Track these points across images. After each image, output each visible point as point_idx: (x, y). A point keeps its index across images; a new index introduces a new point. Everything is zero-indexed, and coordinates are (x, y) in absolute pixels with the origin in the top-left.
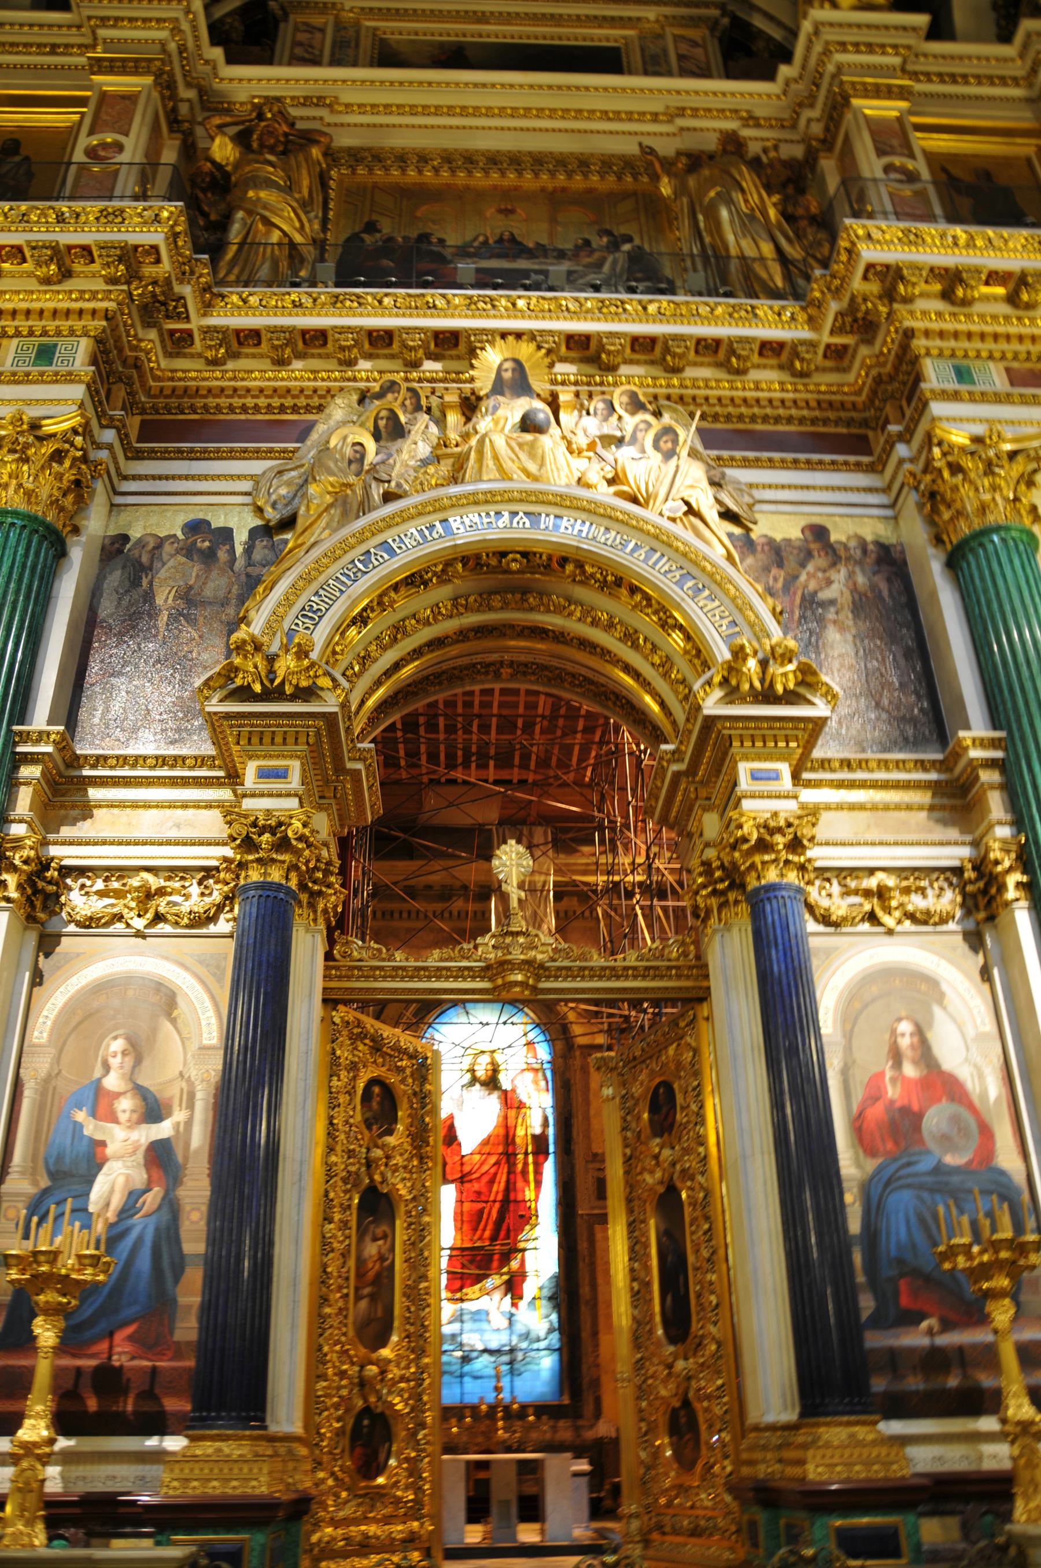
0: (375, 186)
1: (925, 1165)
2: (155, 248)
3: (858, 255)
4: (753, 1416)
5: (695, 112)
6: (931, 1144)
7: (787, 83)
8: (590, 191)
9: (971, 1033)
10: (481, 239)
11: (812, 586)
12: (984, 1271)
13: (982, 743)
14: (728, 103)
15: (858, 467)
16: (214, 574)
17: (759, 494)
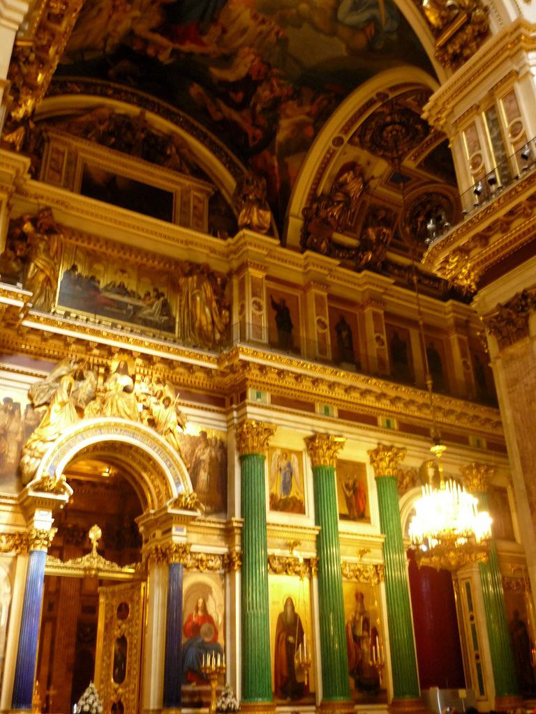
0: (77, 247)
1: (200, 641)
2: (18, 307)
3: (238, 355)
4: (145, 707)
5: (196, 244)
6: (202, 636)
7: (229, 245)
8: (153, 268)
9: (217, 604)
10: (113, 284)
11: (199, 454)
12: (212, 673)
13: (237, 522)
14: (209, 244)
15: (220, 412)
16: (14, 420)
17: (189, 417)
